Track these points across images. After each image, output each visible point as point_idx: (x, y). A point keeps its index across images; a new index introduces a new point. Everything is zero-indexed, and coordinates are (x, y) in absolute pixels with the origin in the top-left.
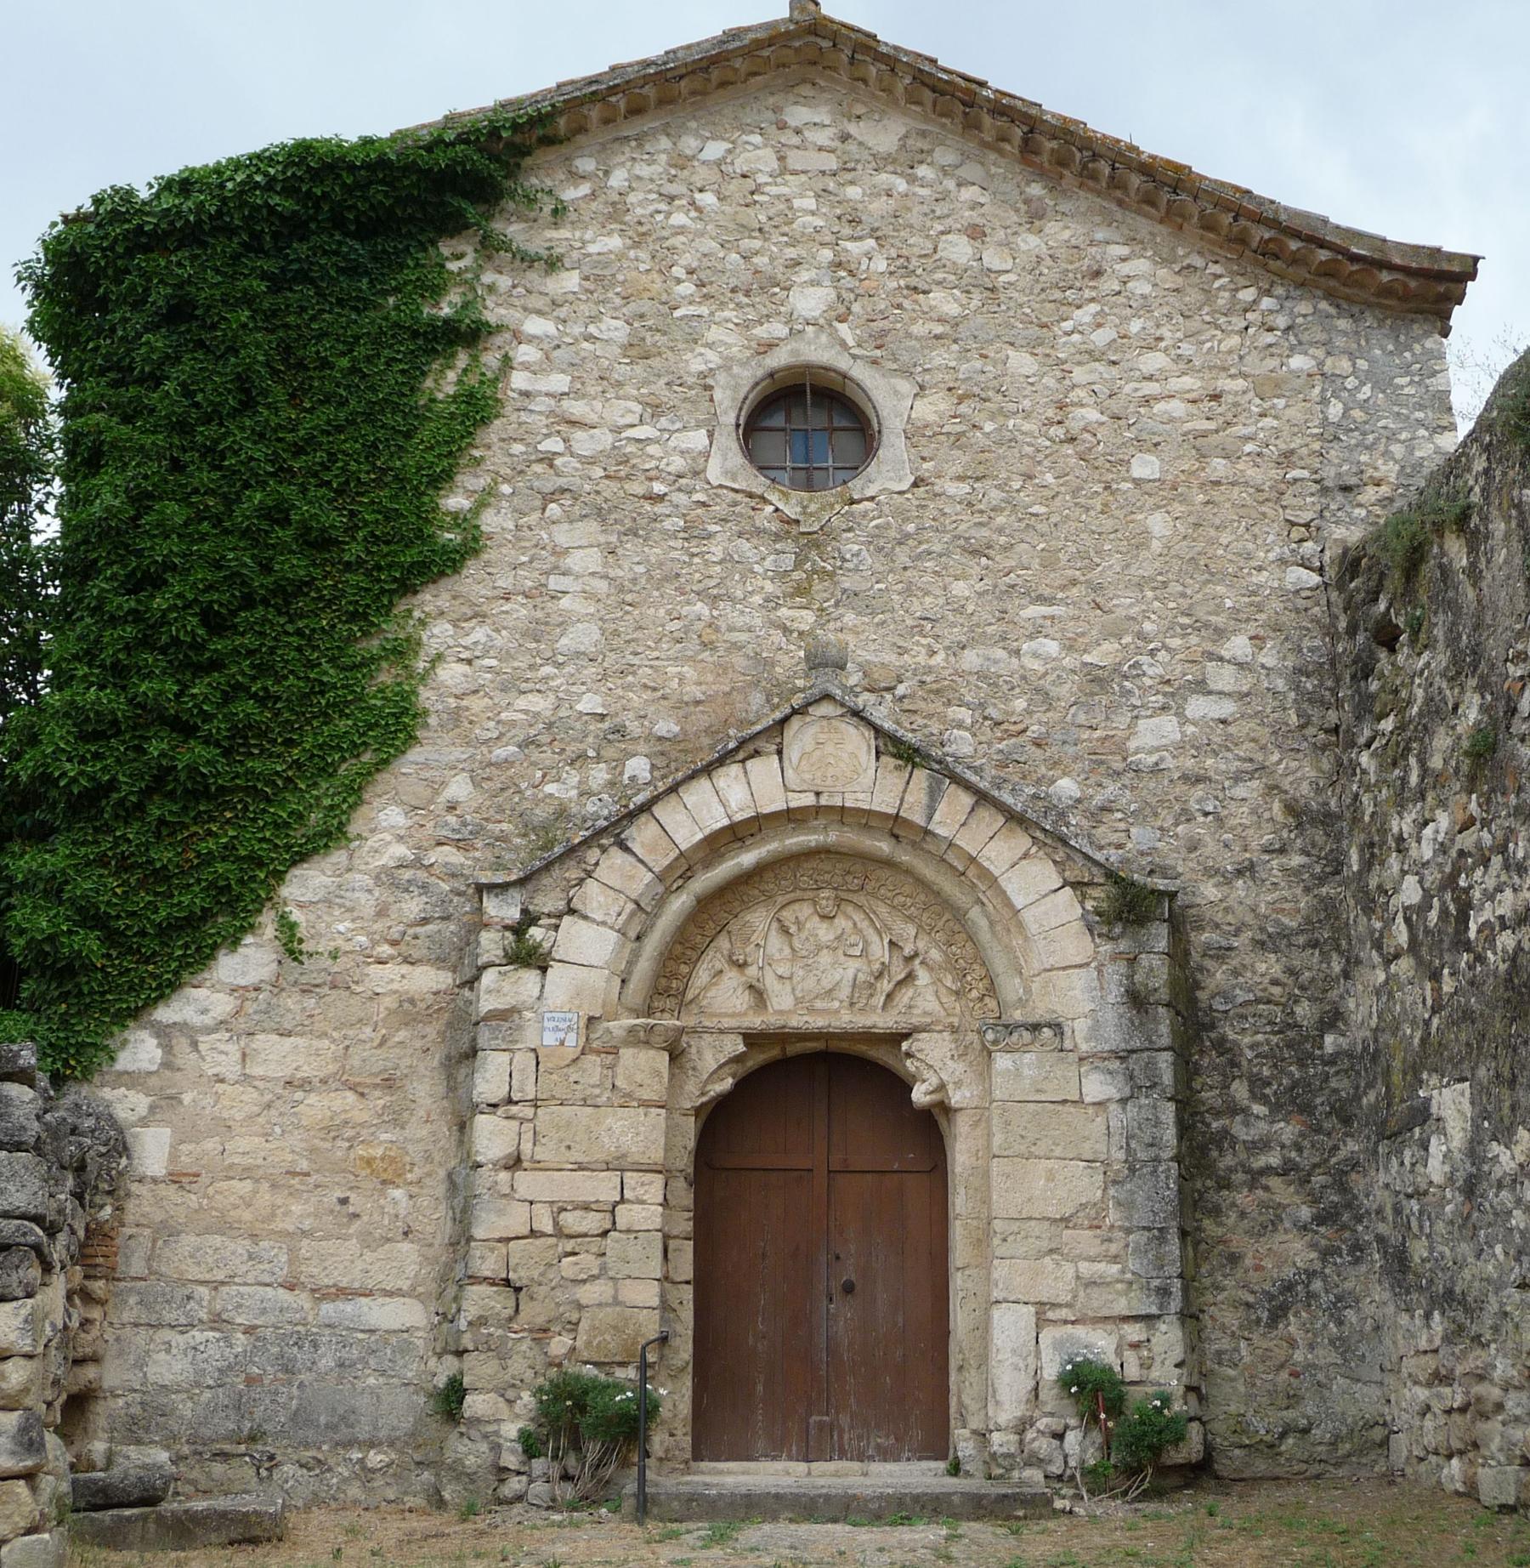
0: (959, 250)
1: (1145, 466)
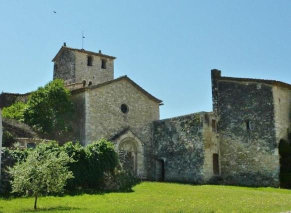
0: (133, 95)
1: (143, 113)
